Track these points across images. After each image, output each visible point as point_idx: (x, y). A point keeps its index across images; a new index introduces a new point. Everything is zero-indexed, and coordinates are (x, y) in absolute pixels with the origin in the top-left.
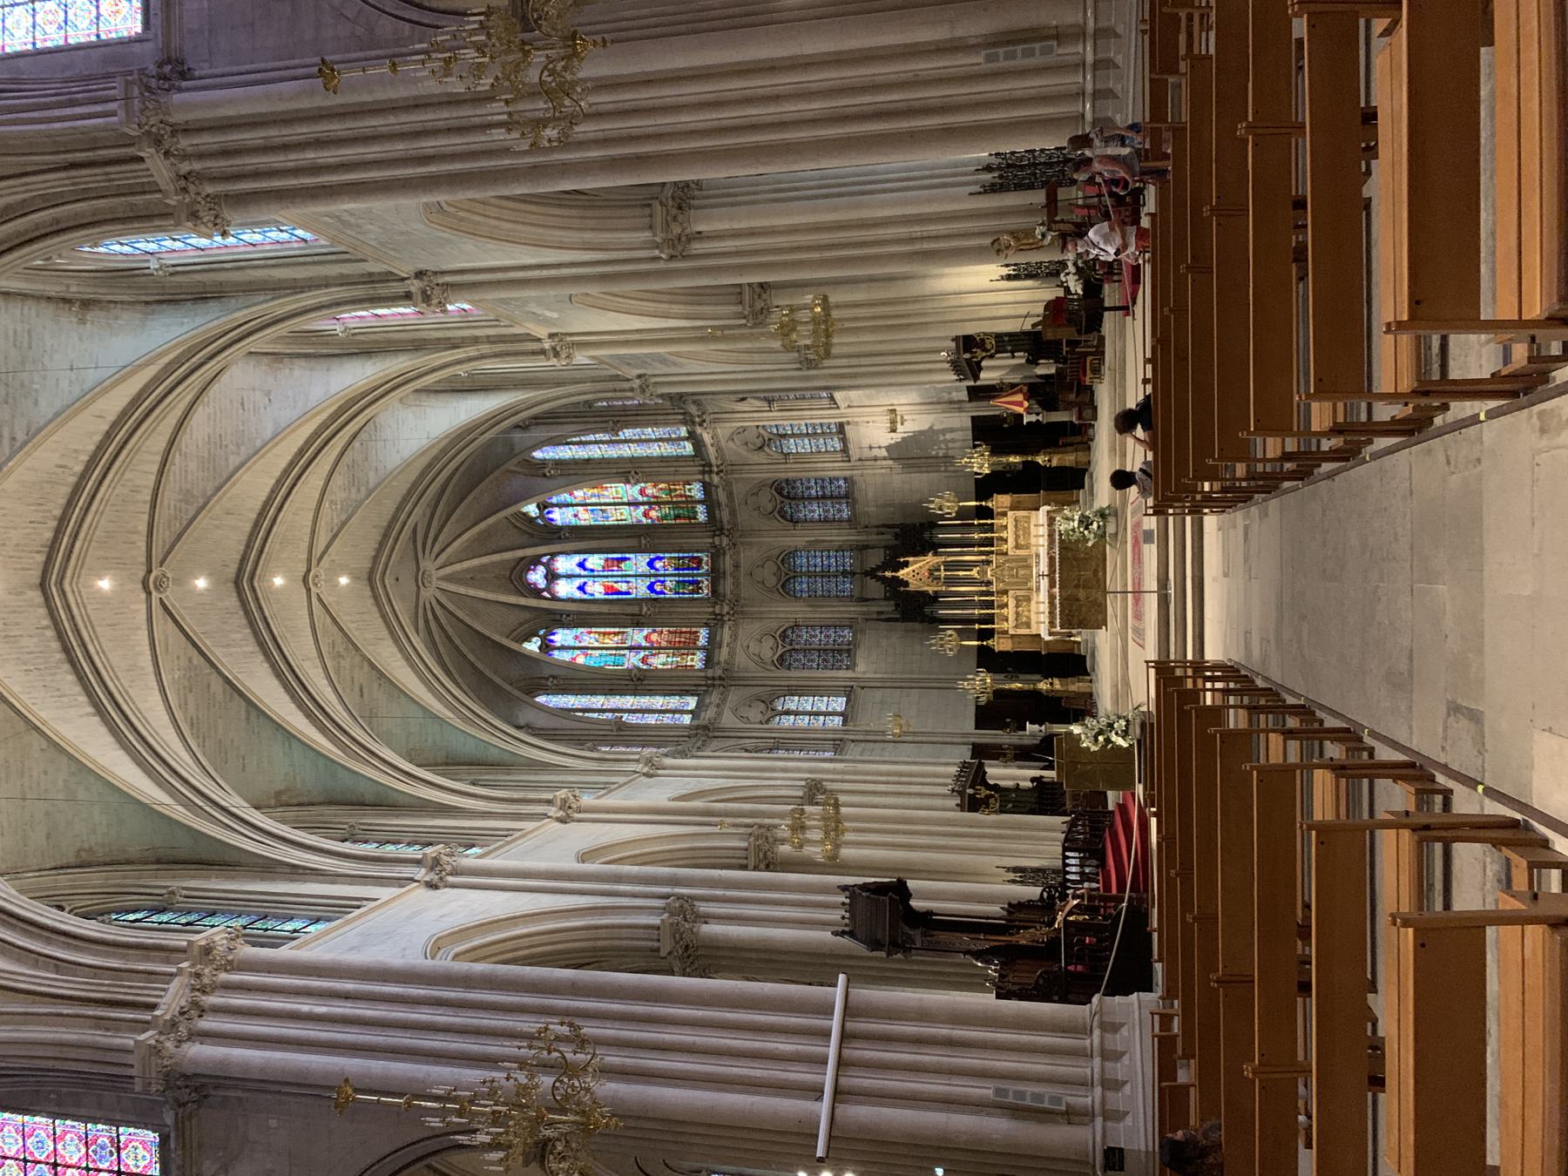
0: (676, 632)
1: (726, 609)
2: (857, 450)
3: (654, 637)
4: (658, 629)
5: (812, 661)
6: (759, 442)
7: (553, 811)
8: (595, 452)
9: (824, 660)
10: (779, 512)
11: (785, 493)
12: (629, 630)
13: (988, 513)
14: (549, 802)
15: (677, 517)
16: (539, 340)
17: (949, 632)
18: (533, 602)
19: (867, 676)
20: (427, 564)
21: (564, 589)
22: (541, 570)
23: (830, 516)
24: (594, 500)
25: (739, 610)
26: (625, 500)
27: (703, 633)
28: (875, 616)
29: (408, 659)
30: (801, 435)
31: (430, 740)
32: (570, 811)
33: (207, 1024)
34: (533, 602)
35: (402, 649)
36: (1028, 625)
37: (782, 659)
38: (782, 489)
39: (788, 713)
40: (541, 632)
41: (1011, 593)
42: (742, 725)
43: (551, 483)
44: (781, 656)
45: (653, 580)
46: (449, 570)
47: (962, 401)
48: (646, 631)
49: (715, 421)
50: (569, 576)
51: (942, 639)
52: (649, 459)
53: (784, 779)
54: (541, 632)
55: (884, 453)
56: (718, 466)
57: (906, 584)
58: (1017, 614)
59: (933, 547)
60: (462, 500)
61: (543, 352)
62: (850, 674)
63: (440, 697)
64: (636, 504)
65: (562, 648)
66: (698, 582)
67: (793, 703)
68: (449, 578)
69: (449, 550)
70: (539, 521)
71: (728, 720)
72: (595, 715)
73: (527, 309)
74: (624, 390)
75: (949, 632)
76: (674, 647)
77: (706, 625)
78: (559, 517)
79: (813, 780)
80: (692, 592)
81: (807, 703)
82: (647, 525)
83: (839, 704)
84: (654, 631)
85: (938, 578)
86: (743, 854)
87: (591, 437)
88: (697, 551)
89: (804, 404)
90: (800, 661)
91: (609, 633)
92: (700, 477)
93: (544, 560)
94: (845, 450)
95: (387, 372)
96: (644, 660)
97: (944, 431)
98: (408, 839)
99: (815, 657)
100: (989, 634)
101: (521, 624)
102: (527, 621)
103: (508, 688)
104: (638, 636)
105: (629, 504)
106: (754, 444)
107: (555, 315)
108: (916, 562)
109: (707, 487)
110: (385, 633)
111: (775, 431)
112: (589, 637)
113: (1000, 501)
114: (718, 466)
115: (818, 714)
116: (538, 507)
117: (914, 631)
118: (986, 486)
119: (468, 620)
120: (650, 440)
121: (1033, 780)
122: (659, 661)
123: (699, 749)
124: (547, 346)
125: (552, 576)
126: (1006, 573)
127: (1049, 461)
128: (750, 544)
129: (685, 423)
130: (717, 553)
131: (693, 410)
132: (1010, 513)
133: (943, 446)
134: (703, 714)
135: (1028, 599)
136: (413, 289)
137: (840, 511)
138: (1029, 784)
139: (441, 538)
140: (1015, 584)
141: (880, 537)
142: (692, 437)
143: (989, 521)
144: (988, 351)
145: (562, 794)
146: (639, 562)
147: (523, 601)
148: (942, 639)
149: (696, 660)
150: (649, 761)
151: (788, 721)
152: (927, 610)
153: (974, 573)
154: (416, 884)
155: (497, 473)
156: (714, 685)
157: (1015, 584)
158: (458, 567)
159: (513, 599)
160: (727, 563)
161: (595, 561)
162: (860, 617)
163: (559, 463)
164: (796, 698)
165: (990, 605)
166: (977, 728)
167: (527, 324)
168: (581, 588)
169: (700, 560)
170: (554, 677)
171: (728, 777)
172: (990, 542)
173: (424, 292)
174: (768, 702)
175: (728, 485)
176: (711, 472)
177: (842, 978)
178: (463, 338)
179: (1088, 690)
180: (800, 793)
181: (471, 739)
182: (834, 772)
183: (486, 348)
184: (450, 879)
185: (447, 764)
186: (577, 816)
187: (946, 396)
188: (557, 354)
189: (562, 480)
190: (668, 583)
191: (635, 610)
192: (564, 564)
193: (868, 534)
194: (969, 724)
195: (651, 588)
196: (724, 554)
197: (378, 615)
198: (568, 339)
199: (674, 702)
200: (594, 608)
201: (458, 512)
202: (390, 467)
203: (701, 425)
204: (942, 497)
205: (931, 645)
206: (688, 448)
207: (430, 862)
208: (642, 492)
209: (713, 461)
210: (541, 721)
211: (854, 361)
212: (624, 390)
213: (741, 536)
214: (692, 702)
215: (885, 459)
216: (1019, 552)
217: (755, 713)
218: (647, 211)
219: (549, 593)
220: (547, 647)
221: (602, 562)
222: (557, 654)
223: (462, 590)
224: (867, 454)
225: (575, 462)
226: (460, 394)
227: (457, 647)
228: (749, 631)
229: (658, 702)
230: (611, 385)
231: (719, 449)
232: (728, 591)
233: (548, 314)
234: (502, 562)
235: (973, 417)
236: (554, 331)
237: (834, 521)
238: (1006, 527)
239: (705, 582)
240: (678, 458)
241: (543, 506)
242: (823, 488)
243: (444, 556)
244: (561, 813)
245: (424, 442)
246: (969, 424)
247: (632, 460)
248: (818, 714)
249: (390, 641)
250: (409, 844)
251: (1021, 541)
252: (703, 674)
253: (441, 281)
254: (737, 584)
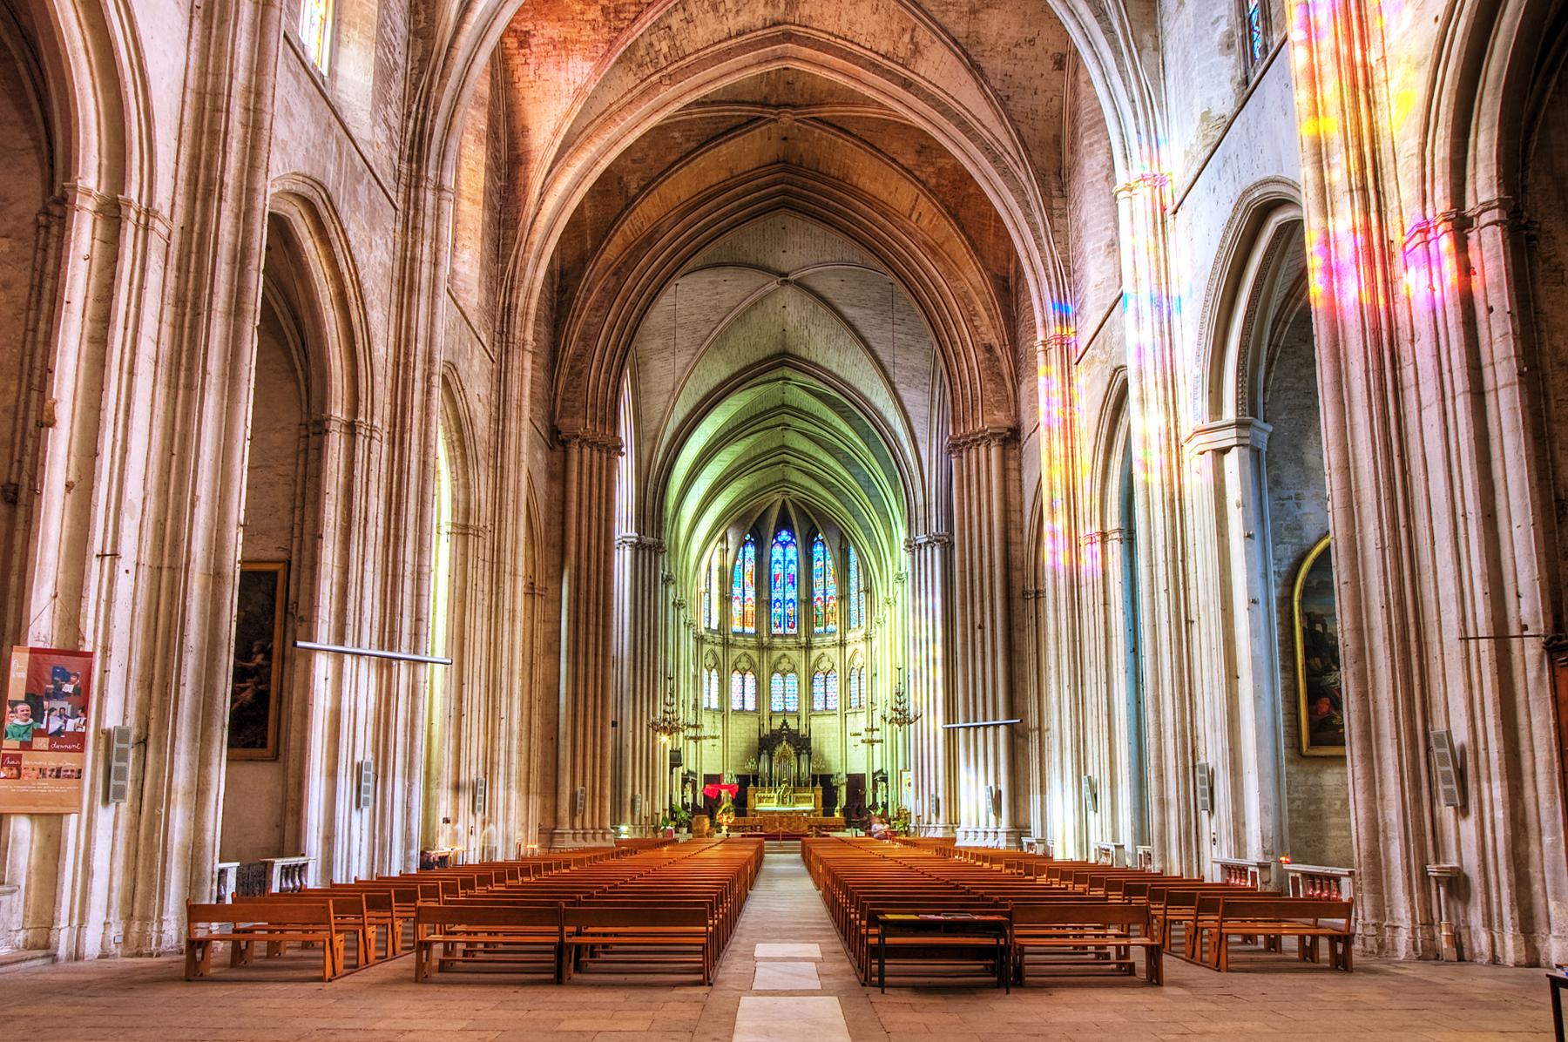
21: (777, 552)
27: (750, 629)
33: (640, 552)
48: (754, 599)
50: (784, 555)
64: (825, 594)
78: (818, 549)
125: (784, 545)
149: (737, 627)
161: (793, 569)
168: (778, 562)
192: (791, 552)
195: (778, 600)
200: (766, 571)
208: (831, 598)
225: (848, 563)
239: (780, 631)
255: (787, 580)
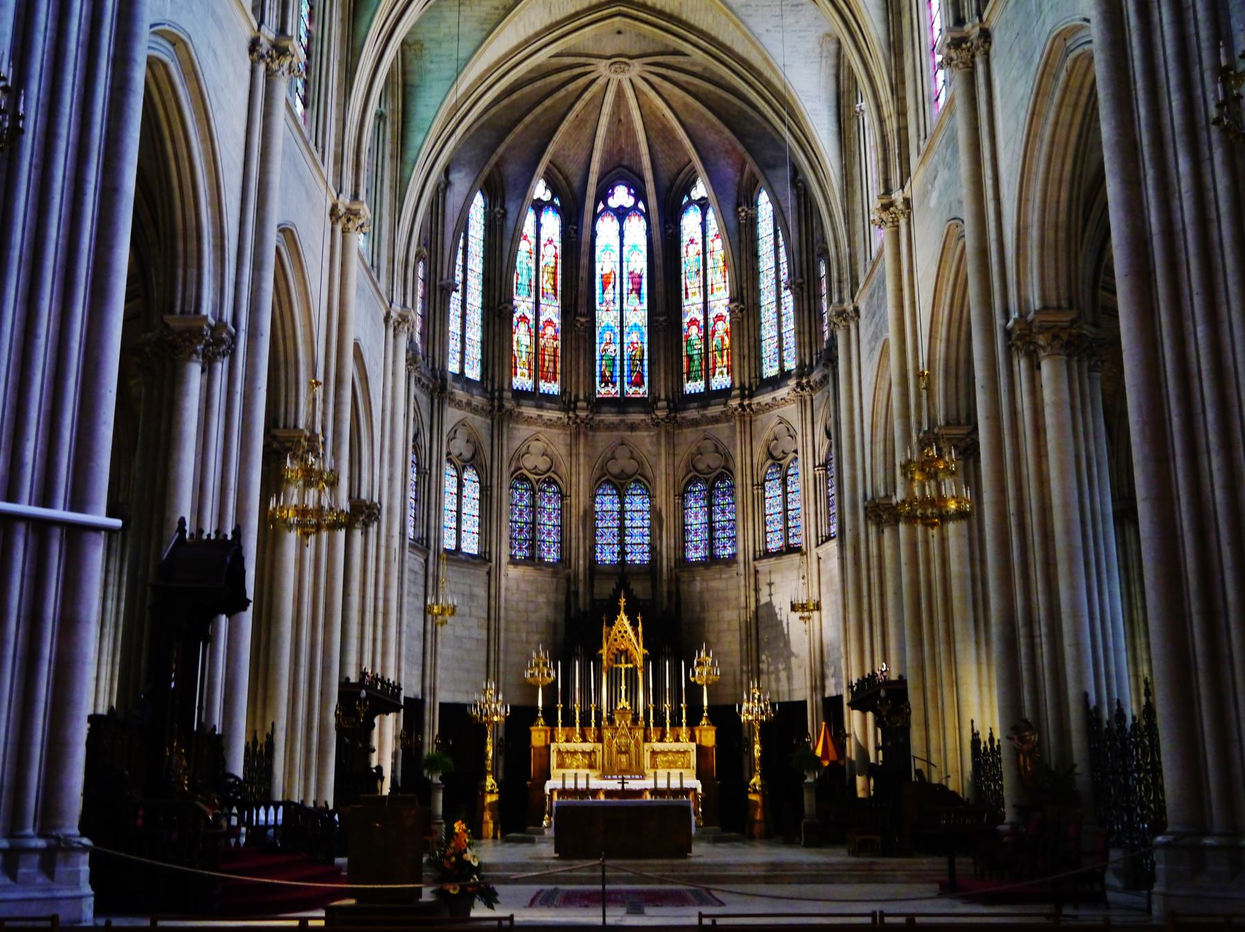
0: (555, 356)
1: (582, 414)
2: (767, 569)
3: (550, 331)
4: (559, 335)
5: (521, 515)
6: (777, 453)
7: (345, 201)
8: (766, 262)
9: (521, 529)
10: (695, 477)
11: (718, 484)
12: (558, 303)
13: (693, 722)
14: (355, 196)
15: (690, 358)
16: (902, 187)
17: (553, 674)
18: (591, 190)
19: (503, 578)
20: (636, 68)
21: (607, 228)
22: (629, 202)
23: (691, 537)
24: (710, 263)
25: (580, 430)
26: (710, 298)
27: (553, 388)
28: (573, 588)
29: (527, 42)
30: (785, 502)
31: (433, 66)
32: (344, 219)
34: (591, 190)
35: (538, 35)
36: (561, 765)
37: (523, 479)
38: (723, 481)
39: (460, 485)
40: (557, 201)
41: (599, 746)
42: (447, 428)
43: (731, 216)
44: (527, 479)
45: (617, 330)
46: (630, 93)
47: (823, 688)
48: (557, 321)
49: (803, 402)
51: (545, 664)
52: (758, 326)
53: (381, 478)
54: (557, 201)
55: (764, 599)
56: (750, 405)
57: (611, 623)
58: (575, 753)
59: (654, 656)
60: (710, 108)
61: (888, 191)
62: (505, 559)
63: (482, 78)
65: (538, 226)
66: (614, 384)
67: (472, 491)
68: (620, 94)
69: (652, 94)
70: (686, 199)
71: (452, 415)
72: (459, 261)
73: (940, 168)
74: (840, 291)
75: (553, 674)
76: (538, 352)
77: (563, 391)
78: (690, 222)
79: (380, 511)
80: (603, 375)
81: (471, 508)
82: (681, 323)
83: (471, 545)
84: (556, 332)
85: (617, 661)
86: (291, 423)
87: (783, 258)
88: (650, 382)
89: (822, 505)
90: (521, 499)
91: (555, 279)
92: (737, 385)
93: (641, 205)
94: (767, 554)
95: (864, 10)
96: (523, 318)
97: (788, 668)
98: (313, 30)
99: (526, 518)
100: (551, 722)
101: (566, 178)
102: (569, 184)
103: (494, 159)
104: (551, 311)
105: (705, 302)
106: (775, 447)
107: (933, 203)
108: (636, 635)
109: (725, 393)
110: (558, 15)
111: (790, 472)
112: (551, 254)
113: (708, 737)
114: (750, 405)
115: (459, 520)
116: (703, 198)
117: (555, 633)
118: (725, 717)
119: (571, 116)
120: (780, 326)
121: (379, 768)
122: (522, 337)
123: (418, 380)
124: (897, 196)
125: (621, 214)
126: (623, 740)
127: (755, 791)
128: (658, 444)
129: (801, 366)
130: (645, 405)
131: (816, 376)
132: (693, 745)
133: (772, 668)
134: (458, 386)
135: (591, 766)
136: (968, 27)
137: (696, 548)
138: (374, 763)
139: (667, 85)
140: (610, 752)
141: (665, 595)
142: (784, 375)
143: (684, 721)
144: (888, 719)
145: (365, 210)
146: (638, 313)
147: (593, 179)
148: (545, 664)
149: (522, 381)
150: (404, 319)
151: (450, 485)
152: (579, 649)
153: (623, 703)
154: (256, 26)
155: (740, 147)
156: (492, 399)
157: (610, 752)
158: (633, 103)
159: (595, 167)
160: (636, 417)
161: (638, 263)
162: (571, 571)
163: (753, 222)
164: (477, 495)
165: (585, 722)
166: (441, 704)
167: (921, 171)
169: (639, 383)
170: (504, 215)
171: (383, 411)
172: (660, 722)
173: (964, 39)
174: (474, 461)
175: (726, 417)
176: (743, 397)
177: (118, 523)
178: (904, 98)
179: (485, 834)
180: (364, 496)
181: (433, 114)
182: (389, 537)
183: (892, 125)
184: (262, 68)
185: (405, 86)
186: (339, 228)
187: (830, 671)
188: (886, 207)
189: (733, 225)
190: (612, 348)
191: (582, 309)
192: (636, 228)
193: (670, 580)
194: (444, 696)
196: (647, 413)
197: (579, 8)
198: (903, 222)
199: (474, 352)
200: (584, 261)
201: (697, 105)
202: (750, 21)
203: (799, 384)
204: (713, 664)
205: (538, 653)
206: (770, 370)
207: (284, 43)
208: (719, 318)
209: (756, 400)
210: (454, 199)
211: (874, 562)
212: (840, 291)
213: (667, 433)
214: (473, 373)
215: (757, 600)
216: (647, 756)
217: (460, 446)
218: (1064, 304)
219: (603, 211)
220: (539, 206)
221: (637, 272)
222: (531, 217)
223: (607, 109)
224: (763, 579)
225: (754, 240)
226: (833, 103)
227: (540, 102)
228: (558, 442)
229: (475, 334)
230: (846, 276)
231: (769, 407)
232: (602, 417)
233: (935, 195)
234: (638, 156)
235: (805, 702)
236: (915, 204)
237: (685, 542)
238: (677, 740)
240: (759, 359)
241: (703, 204)
242: (724, 528)
243: (645, 87)
244: (342, 210)
245: (780, 61)
246: (798, 697)
247: (757, 307)
248: (459, 520)
249: (547, 22)
250: (308, 31)
251: (660, 758)
252: (506, 387)
253: (979, 60)
254: (611, 427)
255: (627, 286)
